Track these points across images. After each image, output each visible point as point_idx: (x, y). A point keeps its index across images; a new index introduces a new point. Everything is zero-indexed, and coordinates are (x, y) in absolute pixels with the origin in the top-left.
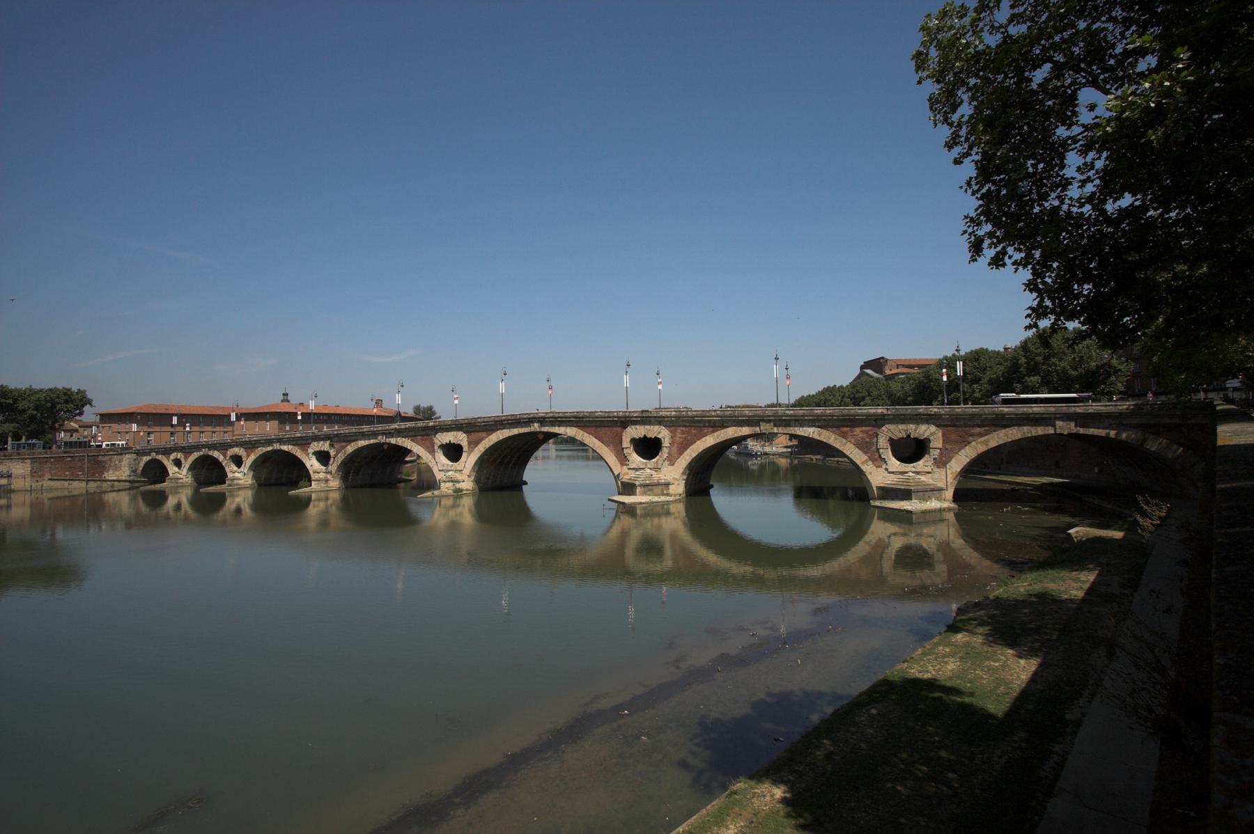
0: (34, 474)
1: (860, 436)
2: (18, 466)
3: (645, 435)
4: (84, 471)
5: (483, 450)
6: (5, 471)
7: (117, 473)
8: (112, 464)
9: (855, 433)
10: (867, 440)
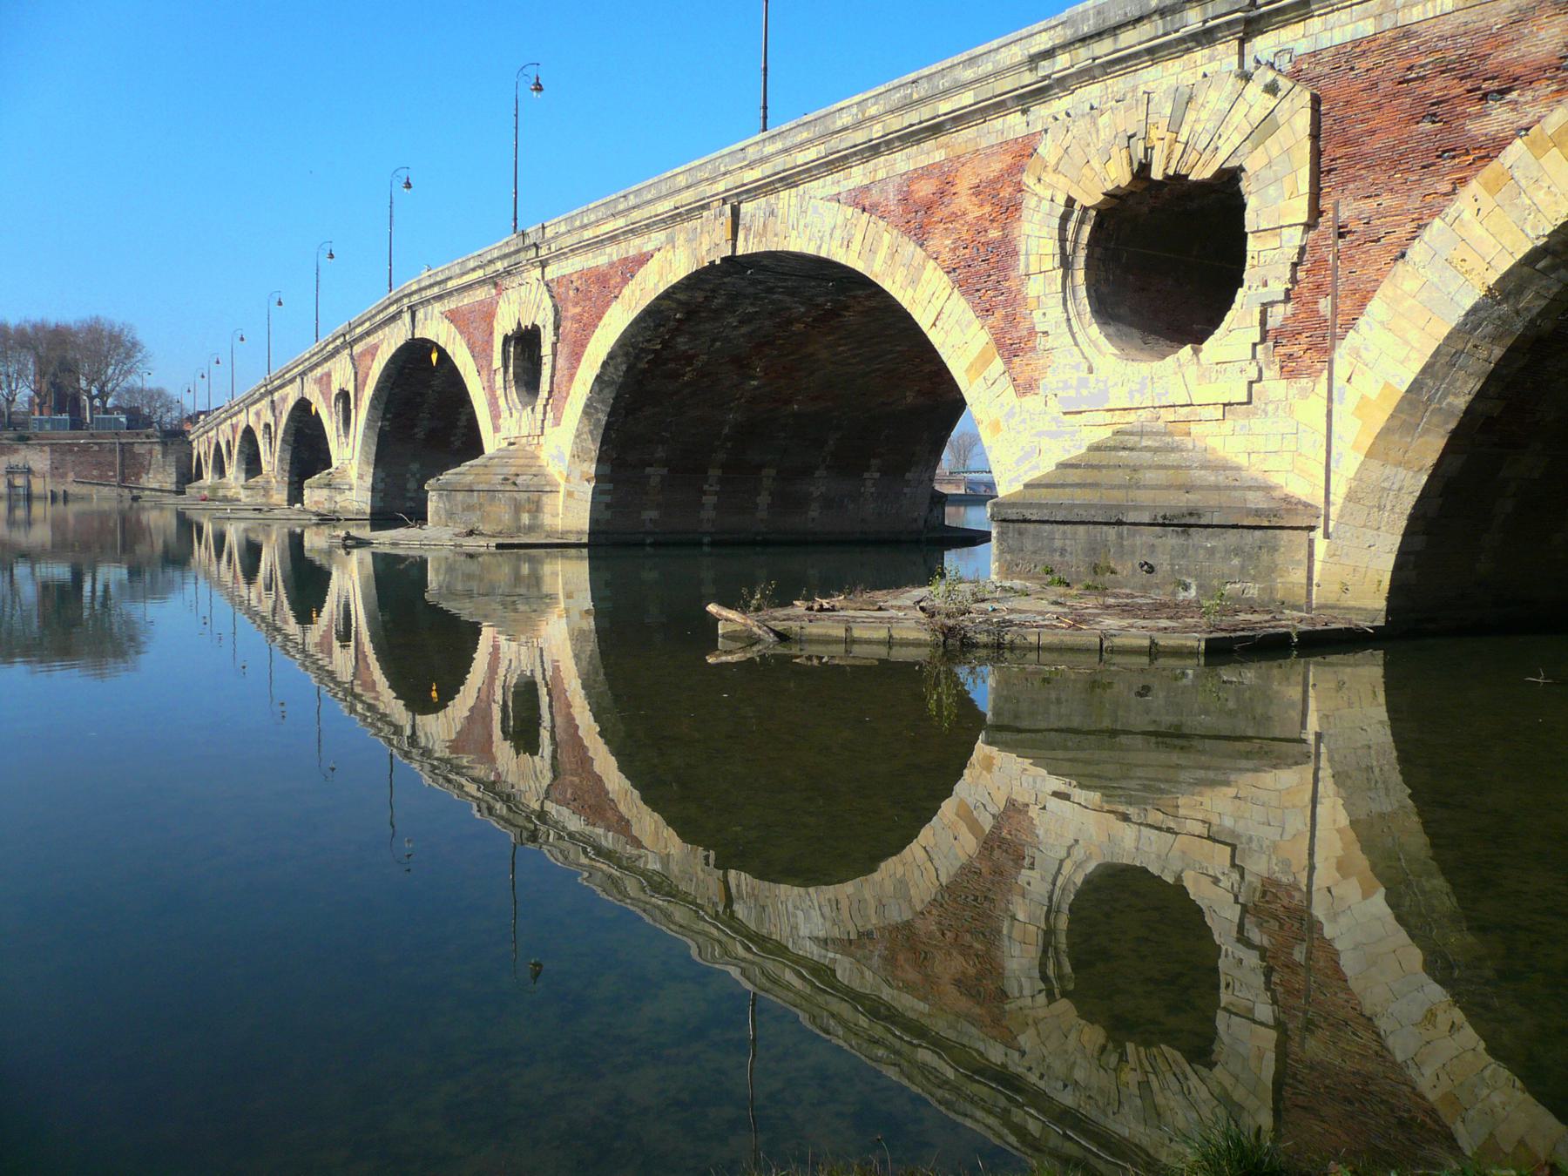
0: (55, 468)
1: (970, 217)
2: (36, 457)
3: (519, 324)
4: (115, 471)
5: (368, 403)
6: (21, 465)
7: (160, 477)
8: (153, 462)
9: (953, 208)
10: (994, 234)
